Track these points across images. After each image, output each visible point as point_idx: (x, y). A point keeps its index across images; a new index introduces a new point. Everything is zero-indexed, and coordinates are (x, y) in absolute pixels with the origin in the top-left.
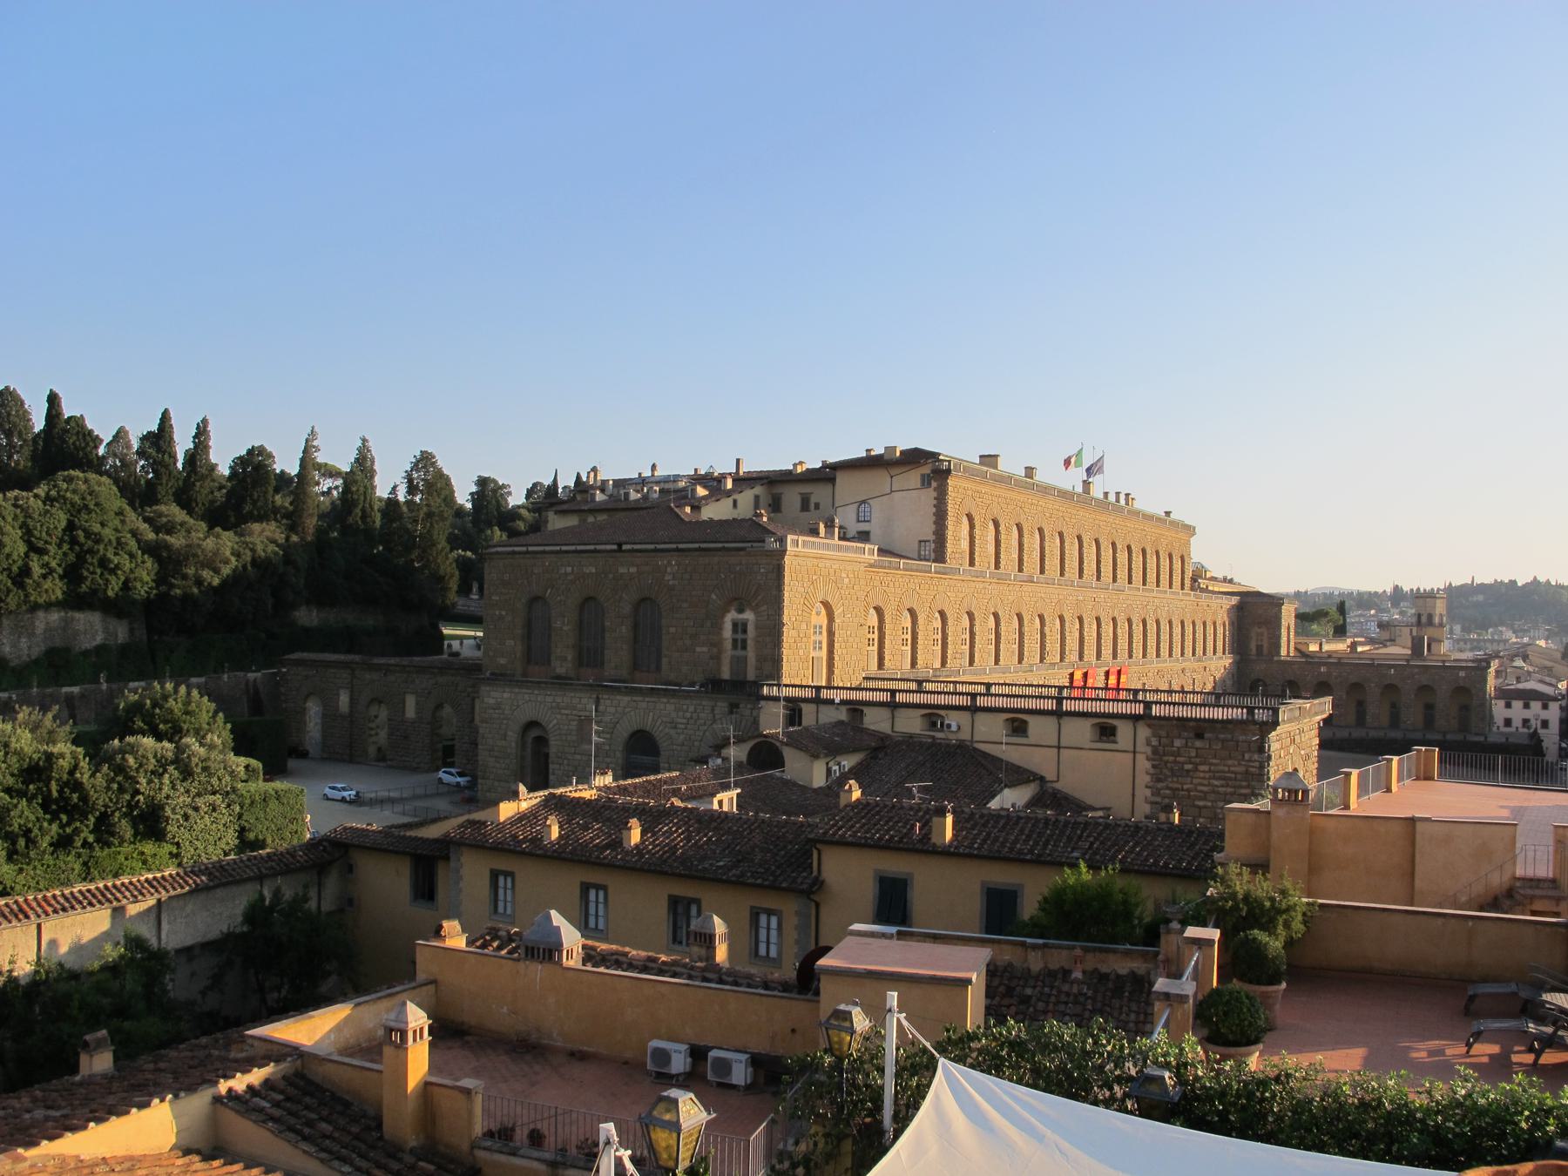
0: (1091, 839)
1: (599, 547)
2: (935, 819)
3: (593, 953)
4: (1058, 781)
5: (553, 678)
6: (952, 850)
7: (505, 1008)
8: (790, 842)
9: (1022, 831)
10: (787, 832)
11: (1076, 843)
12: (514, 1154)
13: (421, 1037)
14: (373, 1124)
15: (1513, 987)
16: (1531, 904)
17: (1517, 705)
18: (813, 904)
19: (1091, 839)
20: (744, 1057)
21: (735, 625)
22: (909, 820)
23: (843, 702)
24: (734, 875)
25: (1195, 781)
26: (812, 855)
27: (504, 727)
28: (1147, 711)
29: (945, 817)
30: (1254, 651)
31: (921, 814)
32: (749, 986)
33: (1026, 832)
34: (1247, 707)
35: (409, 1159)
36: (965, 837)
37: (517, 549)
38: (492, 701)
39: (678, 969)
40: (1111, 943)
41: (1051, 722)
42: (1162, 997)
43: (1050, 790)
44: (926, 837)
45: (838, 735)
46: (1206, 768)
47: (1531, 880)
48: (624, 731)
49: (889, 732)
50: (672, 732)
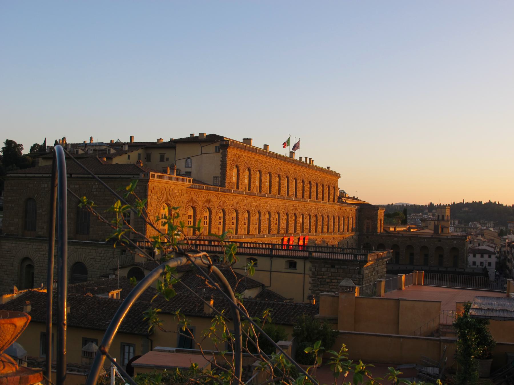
3: (34, 361)
4: (270, 287)
15: (415, 366)
17: (478, 256)
18: (150, 341)
25: (331, 287)
28: (310, 256)
29: (210, 301)
34: (354, 254)
37: (20, 175)
39: (73, 368)
41: (267, 260)
44: (202, 310)
46: (336, 281)
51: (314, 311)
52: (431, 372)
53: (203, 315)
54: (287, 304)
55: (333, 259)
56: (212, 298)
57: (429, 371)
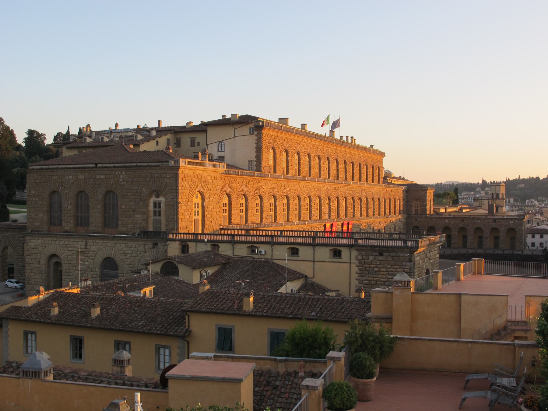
0: (321, 306)
1: (85, 166)
2: (245, 299)
3: (60, 372)
4: (314, 278)
5: (63, 232)
6: (253, 313)
7: (13, 403)
8: (175, 312)
9: (287, 303)
10: (174, 307)
11: (314, 308)
15: (486, 375)
16: (514, 333)
17: (537, 236)
18: (186, 342)
19: (321, 306)
21: (155, 204)
22: (232, 299)
23: (209, 241)
24: (146, 329)
25: (379, 276)
26: (185, 319)
27: (39, 257)
29: (250, 297)
30: (414, 213)
31: (239, 296)
32: (138, 386)
33: (290, 303)
34: (403, 240)
36: (260, 307)
37: (43, 167)
38: (32, 244)
40: (318, 358)
41: (309, 250)
42: (305, 388)
44: (241, 307)
45: (206, 258)
46: (384, 270)
47: (515, 322)
48: (100, 258)
49: (232, 255)
50: (125, 258)
51: (363, 306)
52: (506, 384)
53: (243, 313)
54: (333, 299)
55: (381, 246)
56: (251, 295)
57: (504, 383)
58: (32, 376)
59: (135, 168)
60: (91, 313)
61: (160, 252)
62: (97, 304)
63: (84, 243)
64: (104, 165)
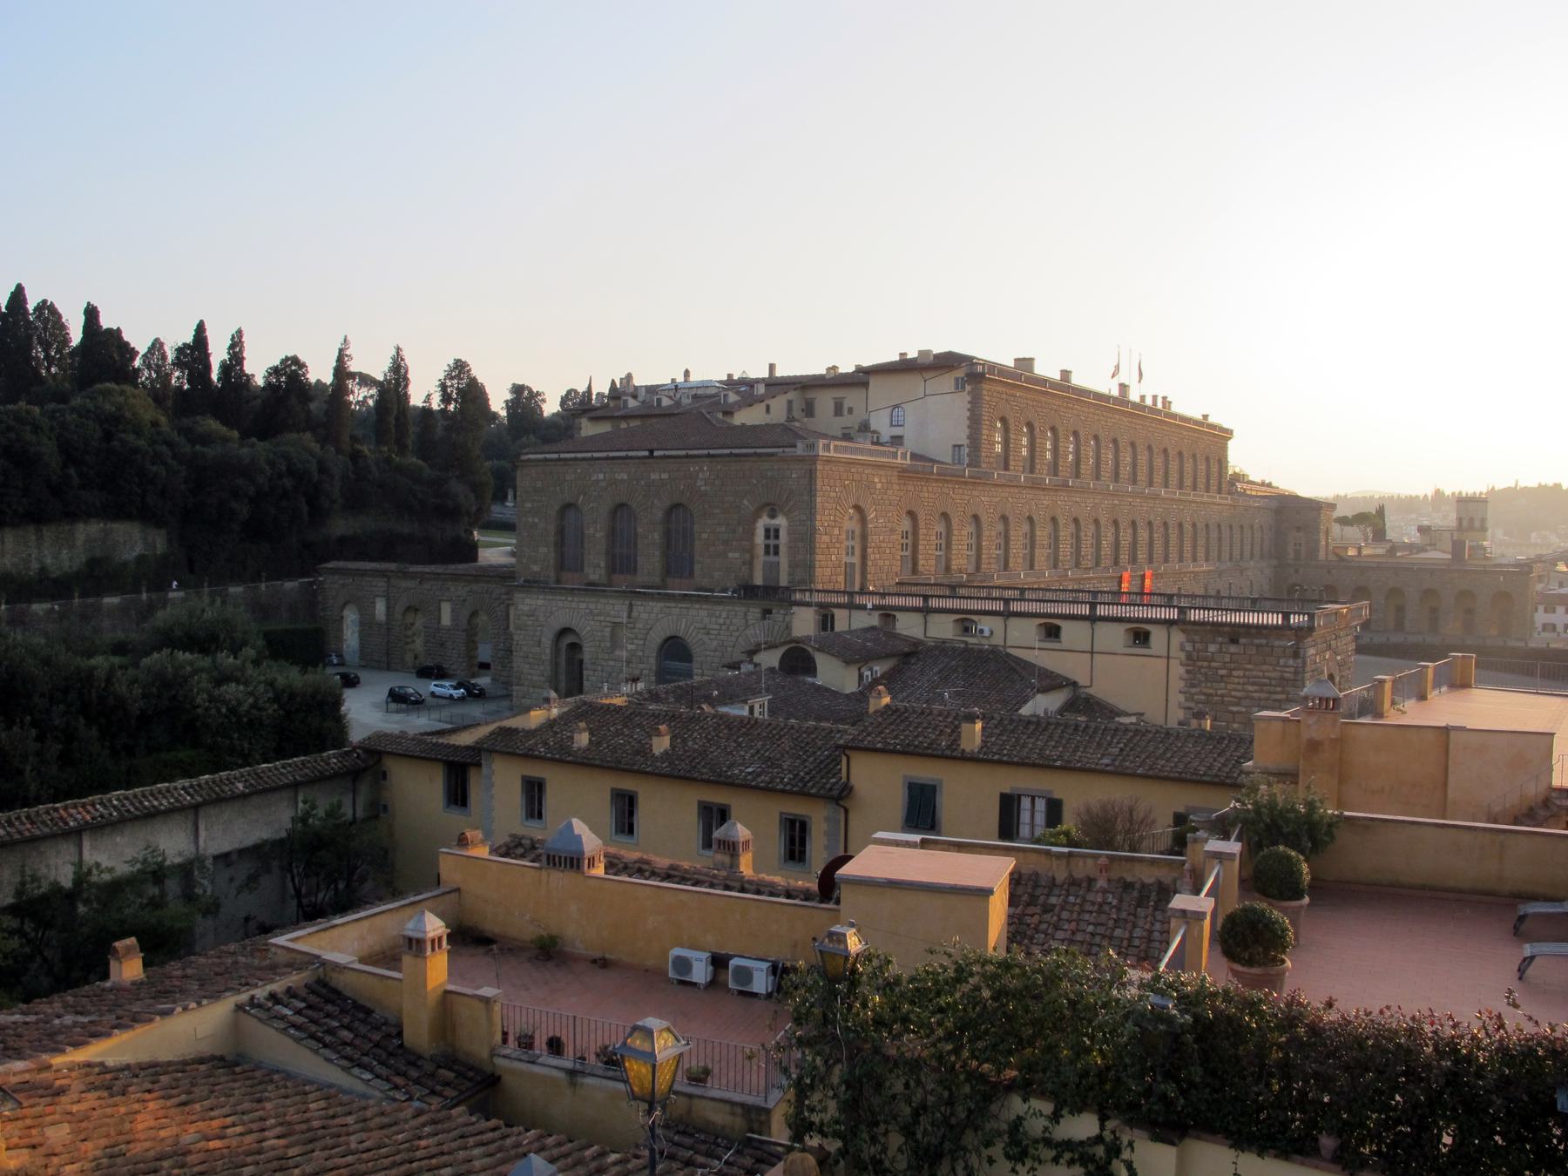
1: (631, 454)
2: (965, 726)
3: (616, 861)
4: (1091, 686)
8: (820, 749)
10: (817, 737)
11: (1107, 749)
12: (533, 1063)
13: (440, 947)
14: (394, 1032)
18: (842, 810)
19: (1121, 745)
20: (765, 965)
21: (767, 531)
23: (875, 608)
24: (762, 782)
25: (1229, 686)
27: (538, 633)
28: (1182, 617)
29: (975, 723)
30: (1291, 555)
31: (949, 720)
32: (772, 894)
34: (1282, 612)
35: (429, 1067)
37: (548, 456)
38: (526, 608)
39: (700, 877)
41: (1085, 626)
43: (1083, 696)
44: (955, 742)
46: (1241, 673)
48: (657, 637)
49: (920, 636)
50: (706, 638)
54: (1147, 731)
58: (565, 866)
59: (728, 459)
60: (651, 745)
61: (777, 627)
62: (663, 728)
63: (625, 608)
64: (667, 453)
